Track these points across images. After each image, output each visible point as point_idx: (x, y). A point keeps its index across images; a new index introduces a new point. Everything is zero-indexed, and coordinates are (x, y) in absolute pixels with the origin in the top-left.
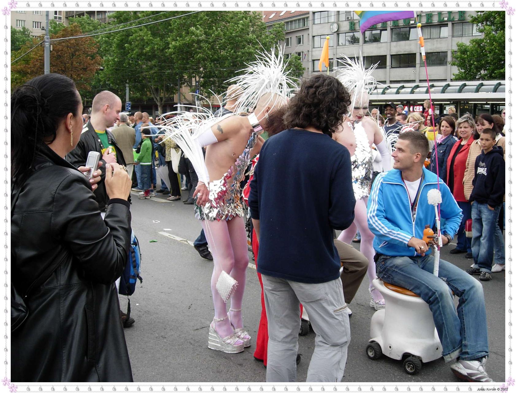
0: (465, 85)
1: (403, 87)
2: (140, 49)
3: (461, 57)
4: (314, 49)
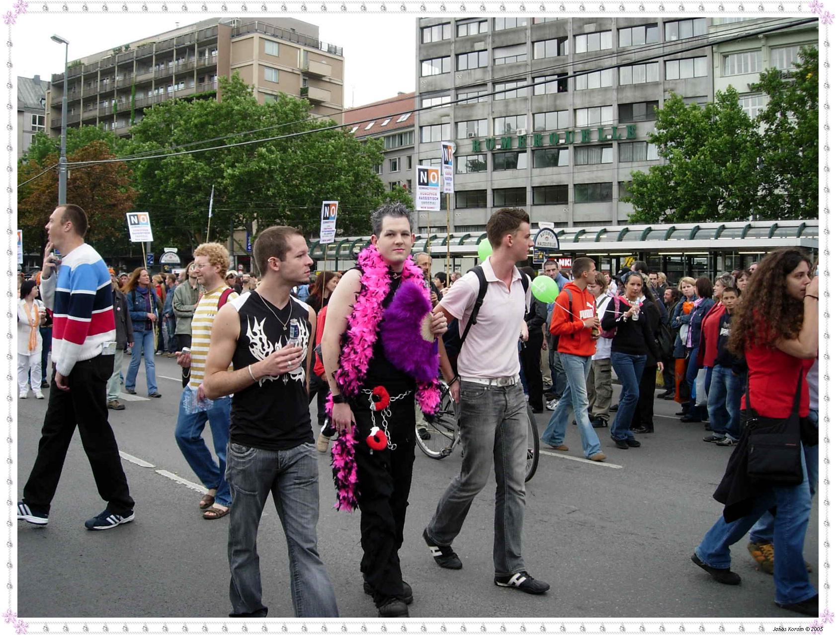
0: (650, 230)
1: (583, 232)
2: (178, 177)
3: (638, 190)
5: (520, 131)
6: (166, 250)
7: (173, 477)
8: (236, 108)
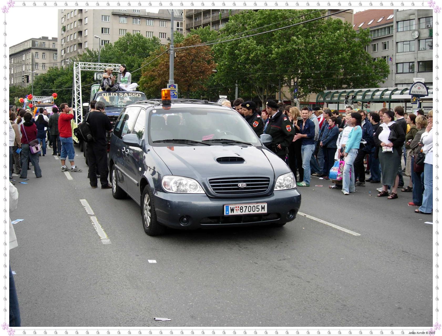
4: (397, 54)
6: (220, 97)
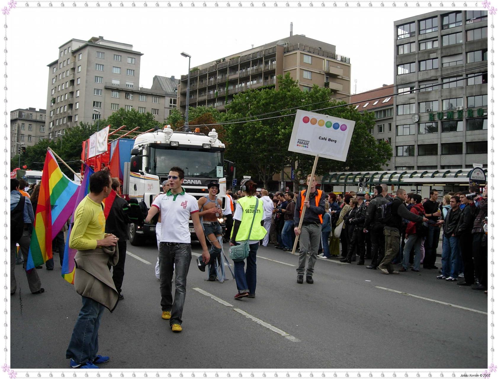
2: (252, 135)
4: (397, 137)
5: (459, 108)
6: (244, 177)
7: (244, 313)
8: (288, 93)
